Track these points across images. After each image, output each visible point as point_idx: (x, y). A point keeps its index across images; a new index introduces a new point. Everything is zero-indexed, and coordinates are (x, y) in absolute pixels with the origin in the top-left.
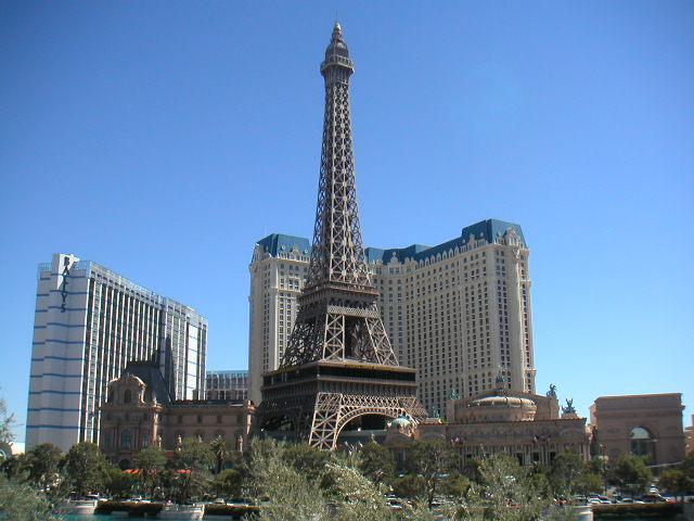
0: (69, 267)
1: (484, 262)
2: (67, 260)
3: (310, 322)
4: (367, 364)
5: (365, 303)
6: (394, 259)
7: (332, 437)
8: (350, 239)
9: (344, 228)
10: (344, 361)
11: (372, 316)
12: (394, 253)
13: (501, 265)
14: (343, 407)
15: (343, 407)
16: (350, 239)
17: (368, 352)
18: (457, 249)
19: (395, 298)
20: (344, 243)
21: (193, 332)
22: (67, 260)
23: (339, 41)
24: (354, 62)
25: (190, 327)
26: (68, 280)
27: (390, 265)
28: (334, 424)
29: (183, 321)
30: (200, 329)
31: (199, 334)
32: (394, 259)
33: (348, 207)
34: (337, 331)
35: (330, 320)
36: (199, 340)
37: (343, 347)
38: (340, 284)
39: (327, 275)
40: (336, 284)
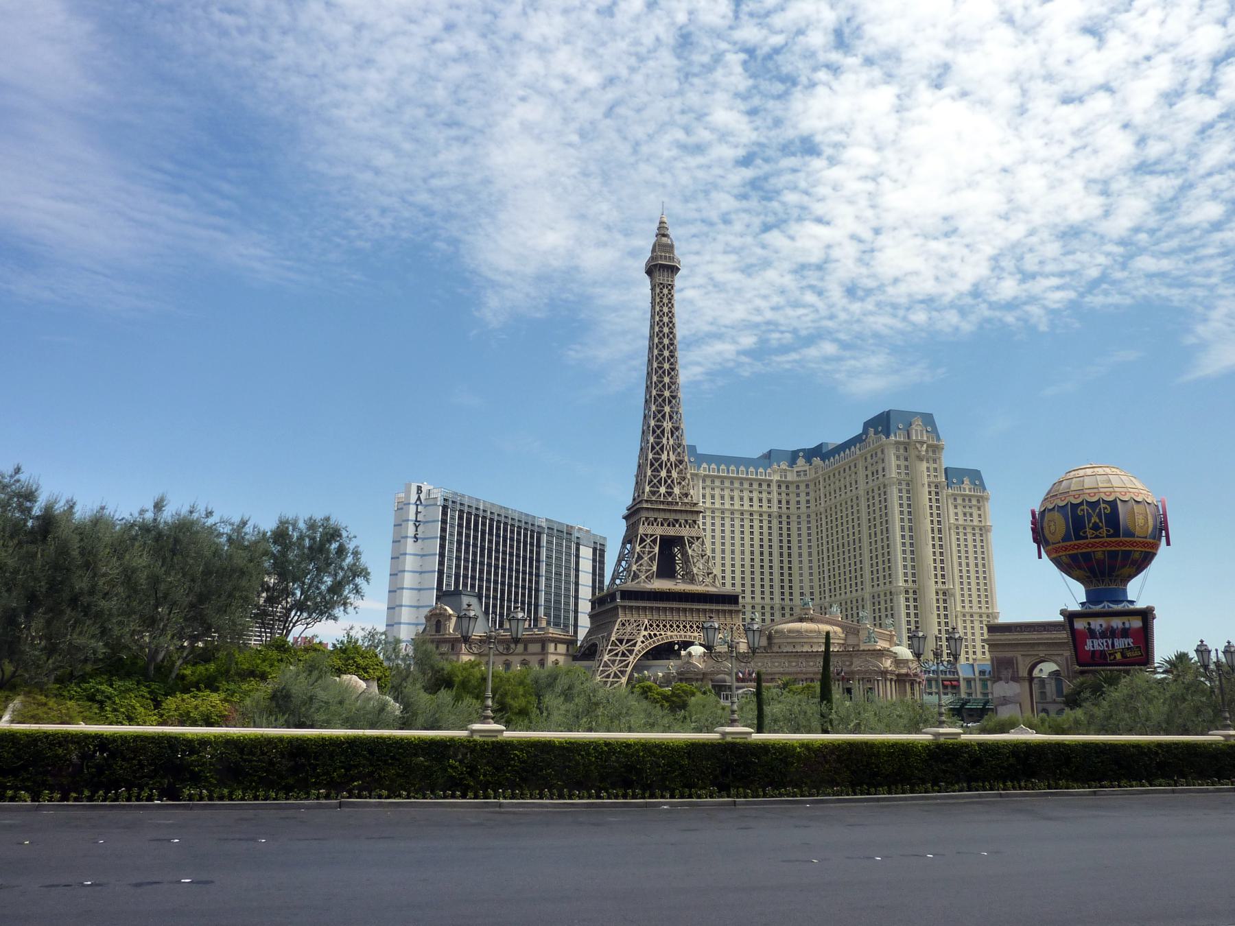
0: (423, 497)
2: (419, 488)
7: (627, 666)
9: (664, 441)
11: (694, 534)
12: (801, 454)
13: (903, 463)
14: (646, 633)
15: (646, 633)
17: (690, 577)
19: (803, 505)
20: (664, 457)
21: (586, 553)
22: (419, 488)
27: (796, 469)
30: (595, 550)
36: (594, 560)
37: (655, 568)
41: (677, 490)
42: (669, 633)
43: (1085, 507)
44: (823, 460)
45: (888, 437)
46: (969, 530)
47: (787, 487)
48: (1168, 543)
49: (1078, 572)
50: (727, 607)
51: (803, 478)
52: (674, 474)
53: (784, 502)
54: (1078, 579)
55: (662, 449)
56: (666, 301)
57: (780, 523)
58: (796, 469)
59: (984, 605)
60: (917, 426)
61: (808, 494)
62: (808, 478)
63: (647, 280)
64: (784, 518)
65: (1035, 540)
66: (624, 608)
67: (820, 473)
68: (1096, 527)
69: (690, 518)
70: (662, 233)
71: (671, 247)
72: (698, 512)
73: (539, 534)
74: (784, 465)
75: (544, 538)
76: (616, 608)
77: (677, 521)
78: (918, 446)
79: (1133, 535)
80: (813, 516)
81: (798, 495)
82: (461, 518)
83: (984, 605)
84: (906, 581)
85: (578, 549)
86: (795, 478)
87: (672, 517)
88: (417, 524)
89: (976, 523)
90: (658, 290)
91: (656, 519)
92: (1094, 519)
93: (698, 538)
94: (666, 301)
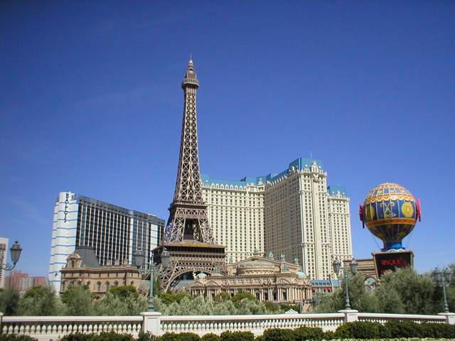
0: (69, 199)
1: (298, 182)
4: (195, 243)
9: (189, 171)
10: (184, 243)
11: (203, 218)
13: (307, 183)
17: (201, 240)
20: (189, 179)
21: (154, 227)
23: (191, 70)
25: (152, 225)
26: (68, 205)
31: (159, 228)
33: (192, 159)
38: (185, 202)
41: (195, 196)
42: (189, 267)
43: (383, 203)
46: (340, 216)
48: (420, 220)
49: (380, 235)
50: (219, 254)
51: (261, 190)
52: (194, 188)
53: (252, 202)
54: (381, 238)
55: (188, 175)
59: (346, 251)
65: (361, 219)
68: (388, 213)
69: (201, 210)
72: (205, 208)
73: (130, 218)
75: (132, 220)
79: (404, 216)
81: (259, 199)
82: (88, 210)
83: (346, 251)
85: (150, 226)
88: (66, 212)
89: (343, 212)
92: (387, 209)
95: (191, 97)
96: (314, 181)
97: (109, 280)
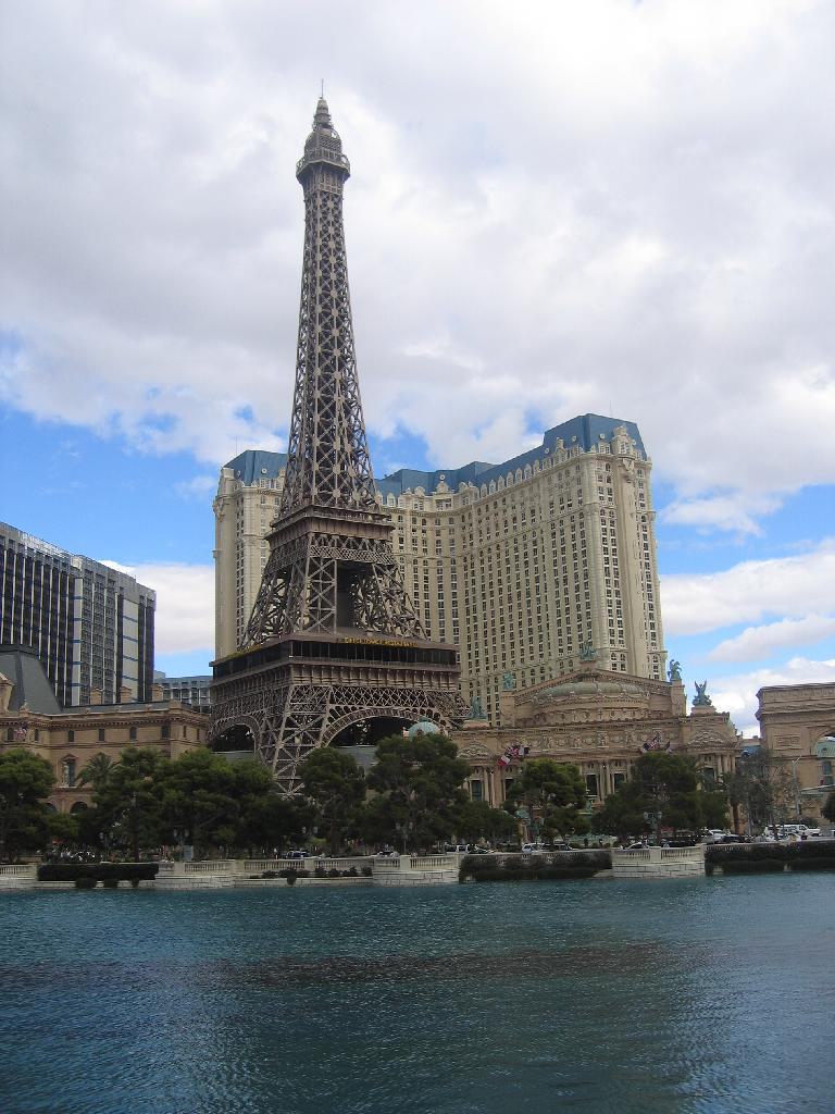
1: (579, 481)
3: (285, 573)
4: (372, 637)
5: (372, 541)
6: (442, 487)
8: (346, 440)
9: (336, 420)
10: (336, 635)
12: (442, 477)
14: (333, 707)
15: (333, 707)
16: (346, 440)
18: (537, 462)
21: (131, 610)
24: (353, 152)
27: (435, 498)
28: (317, 735)
29: (111, 591)
30: (141, 605)
32: (442, 487)
34: (324, 586)
35: (313, 568)
38: (329, 510)
39: (309, 497)
40: (323, 510)
42: (366, 708)
44: (477, 484)
45: (587, 449)
47: (424, 522)
56: (331, 218)
57: (415, 570)
58: (435, 498)
60: (622, 438)
61: (451, 531)
62: (451, 509)
63: (300, 187)
64: (420, 563)
66: (299, 668)
67: (471, 501)
70: (322, 118)
71: (338, 142)
73: (73, 579)
74: (420, 491)
75: (80, 586)
76: (287, 668)
77: (359, 540)
78: (625, 462)
80: (460, 561)
84: (612, 642)
86: (436, 510)
87: (350, 534)
90: (319, 202)
91: (330, 536)
93: (390, 567)
94: (331, 218)
95: (330, 204)
96: (627, 478)
97: (72, 751)
